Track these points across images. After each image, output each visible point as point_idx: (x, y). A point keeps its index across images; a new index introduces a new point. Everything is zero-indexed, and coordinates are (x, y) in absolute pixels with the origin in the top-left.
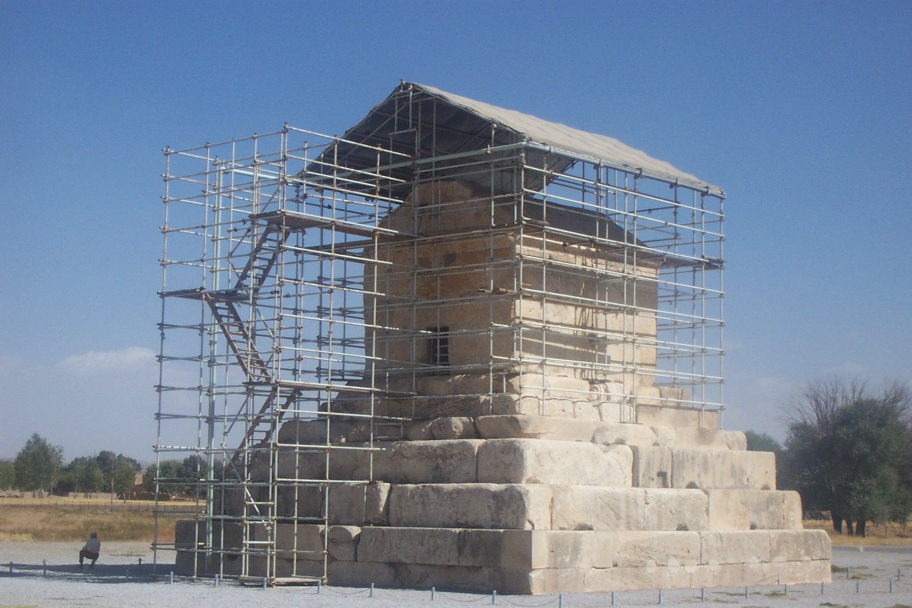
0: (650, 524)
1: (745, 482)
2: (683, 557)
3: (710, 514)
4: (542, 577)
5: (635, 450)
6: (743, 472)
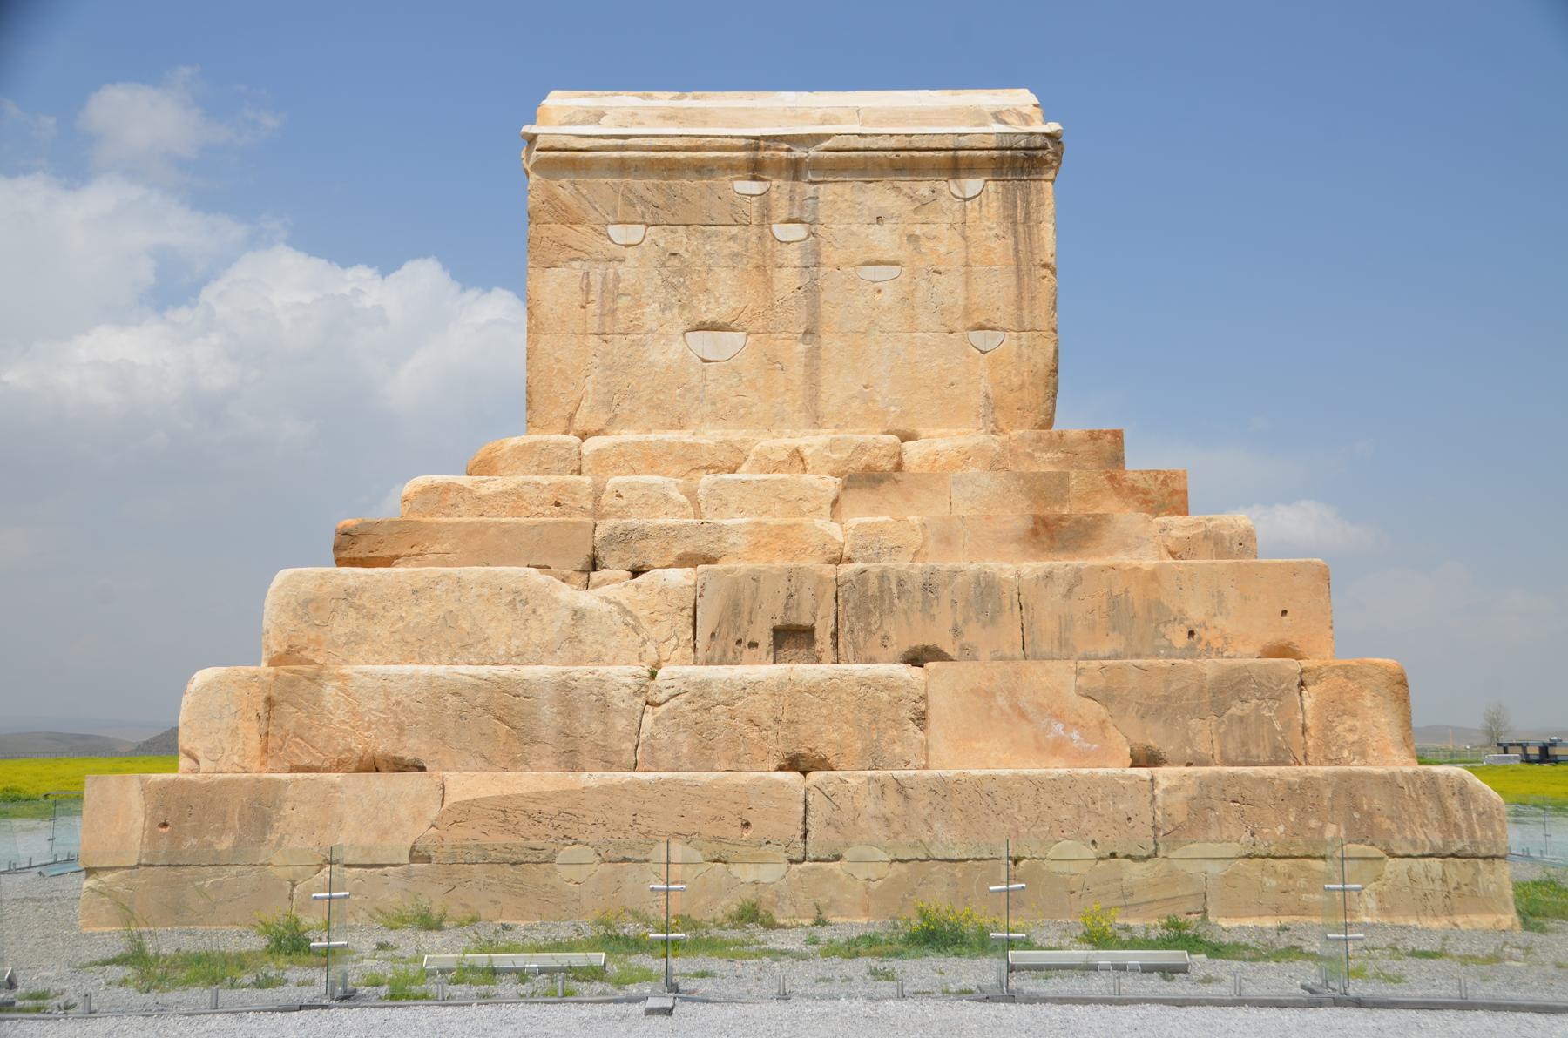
1: (1180, 640)
2: (719, 840)
3: (933, 724)
6: (1159, 616)
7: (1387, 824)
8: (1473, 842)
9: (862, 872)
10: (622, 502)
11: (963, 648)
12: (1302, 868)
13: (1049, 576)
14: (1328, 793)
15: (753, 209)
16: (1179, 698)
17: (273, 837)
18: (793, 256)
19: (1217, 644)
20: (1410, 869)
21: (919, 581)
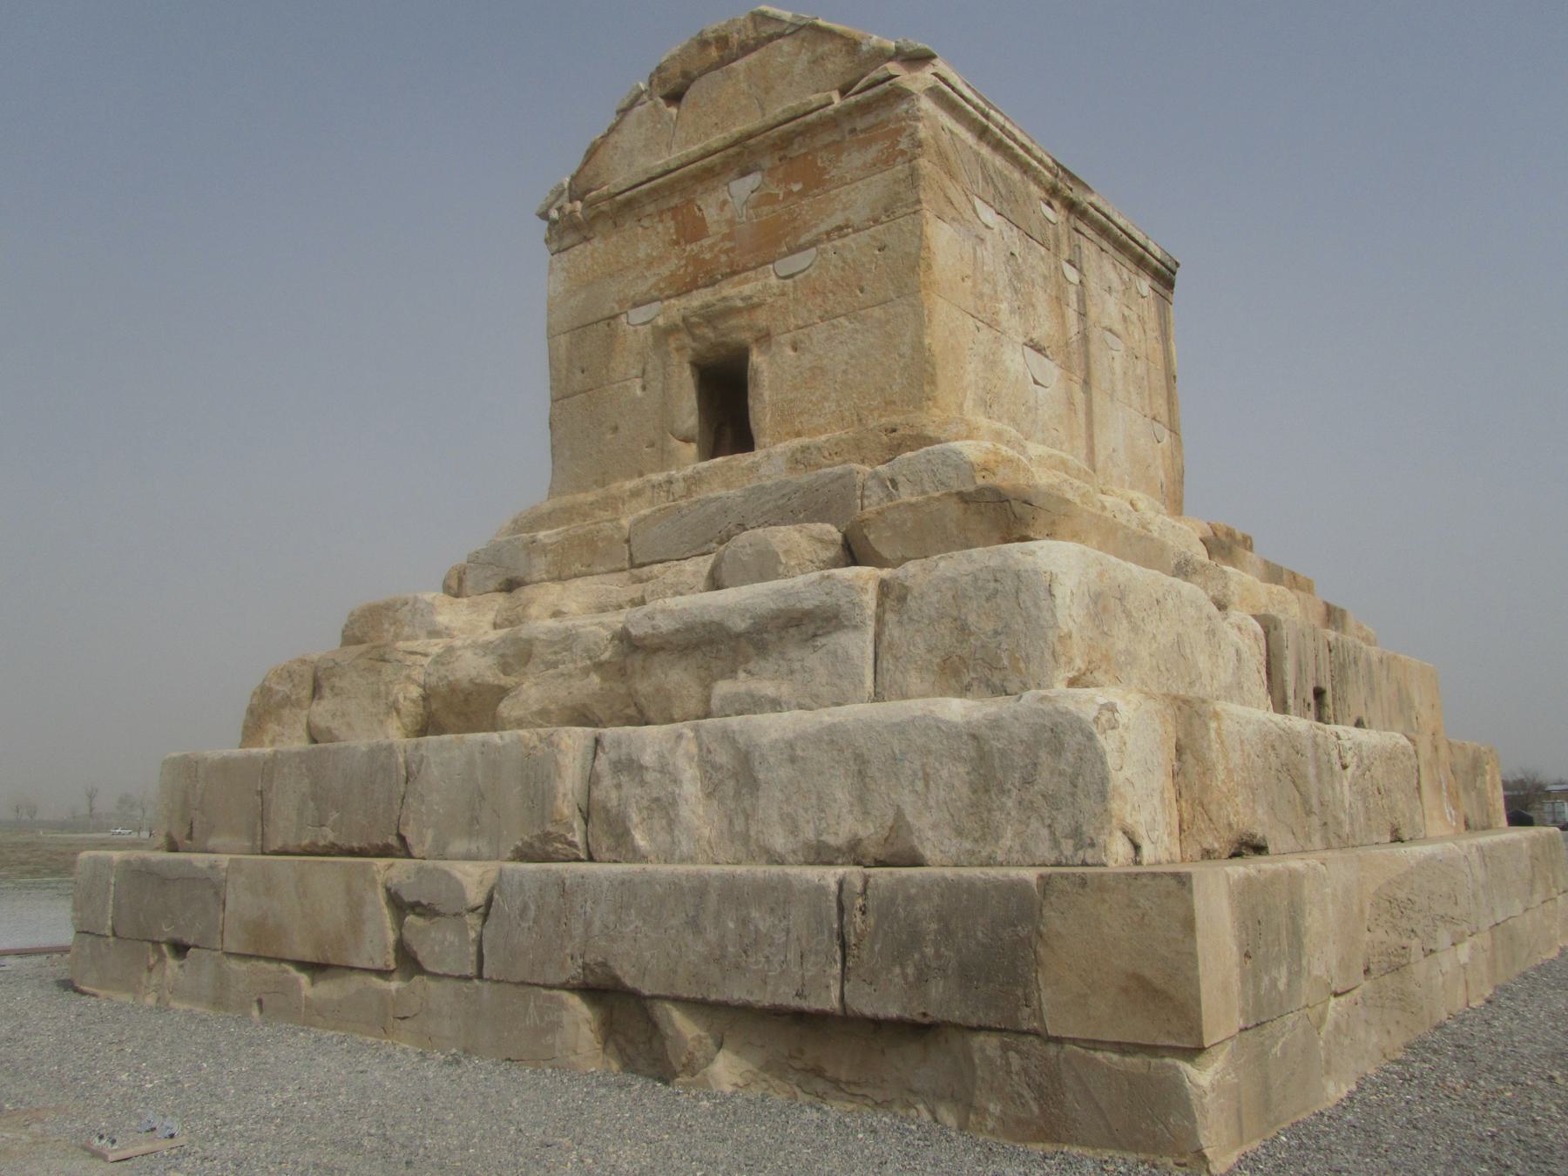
4: (1231, 1078)
5: (1269, 625)
6: (1411, 707)
15: (1050, 233)
17: (1304, 963)
18: (1073, 298)
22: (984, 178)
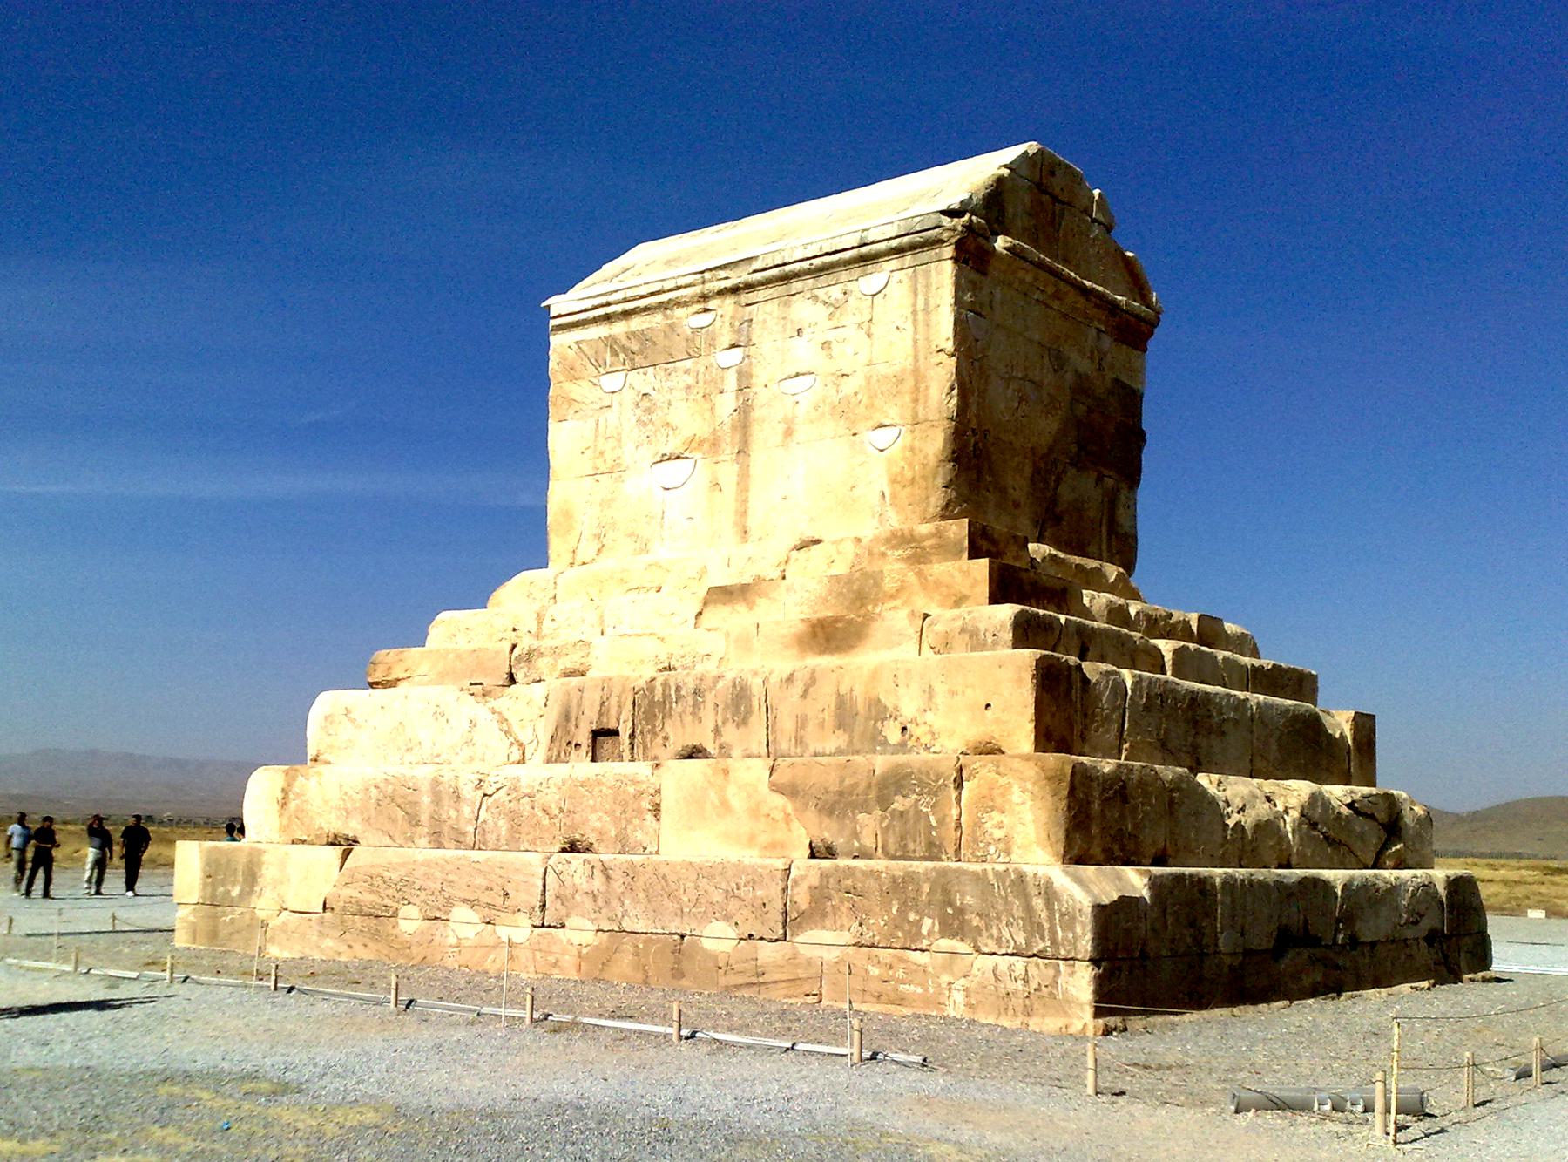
0: (491, 838)
1: (894, 736)
2: (489, 905)
3: (663, 815)
4: (192, 918)
7: (976, 921)
8: (1054, 942)
9: (578, 938)
10: (554, 625)
11: (721, 747)
12: (902, 960)
13: (790, 679)
14: (926, 888)
16: (851, 794)
17: (257, 889)
18: (731, 381)
19: (926, 739)
20: (995, 968)
21: (691, 686)
22: (615, 354)
